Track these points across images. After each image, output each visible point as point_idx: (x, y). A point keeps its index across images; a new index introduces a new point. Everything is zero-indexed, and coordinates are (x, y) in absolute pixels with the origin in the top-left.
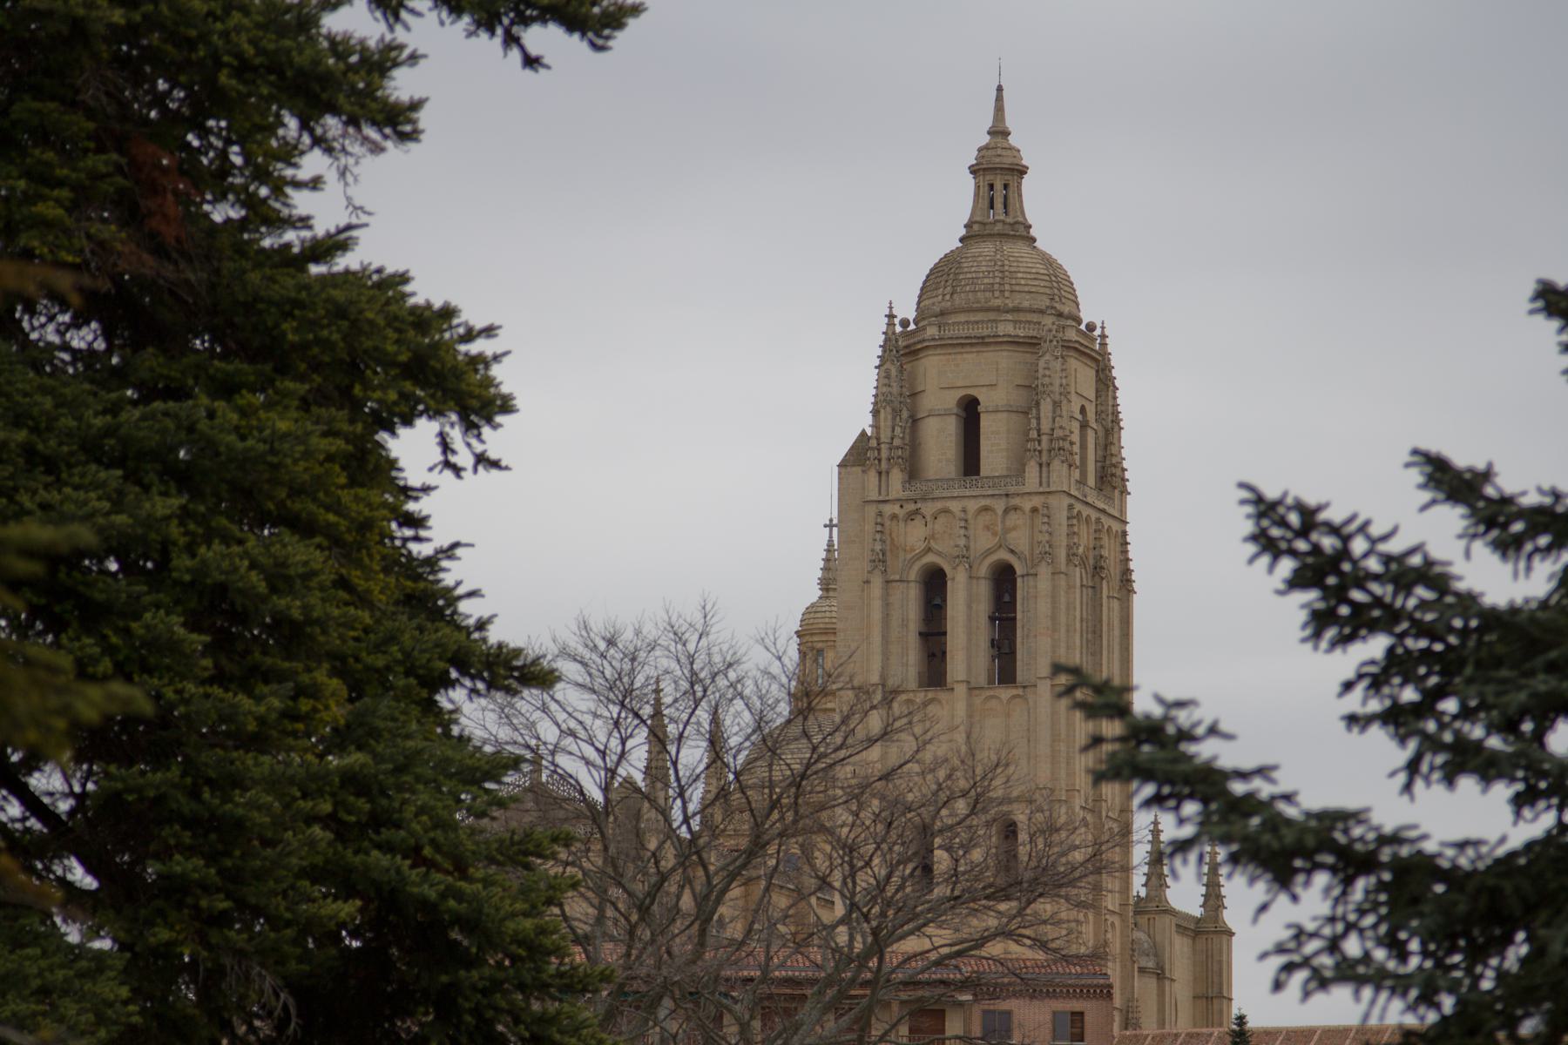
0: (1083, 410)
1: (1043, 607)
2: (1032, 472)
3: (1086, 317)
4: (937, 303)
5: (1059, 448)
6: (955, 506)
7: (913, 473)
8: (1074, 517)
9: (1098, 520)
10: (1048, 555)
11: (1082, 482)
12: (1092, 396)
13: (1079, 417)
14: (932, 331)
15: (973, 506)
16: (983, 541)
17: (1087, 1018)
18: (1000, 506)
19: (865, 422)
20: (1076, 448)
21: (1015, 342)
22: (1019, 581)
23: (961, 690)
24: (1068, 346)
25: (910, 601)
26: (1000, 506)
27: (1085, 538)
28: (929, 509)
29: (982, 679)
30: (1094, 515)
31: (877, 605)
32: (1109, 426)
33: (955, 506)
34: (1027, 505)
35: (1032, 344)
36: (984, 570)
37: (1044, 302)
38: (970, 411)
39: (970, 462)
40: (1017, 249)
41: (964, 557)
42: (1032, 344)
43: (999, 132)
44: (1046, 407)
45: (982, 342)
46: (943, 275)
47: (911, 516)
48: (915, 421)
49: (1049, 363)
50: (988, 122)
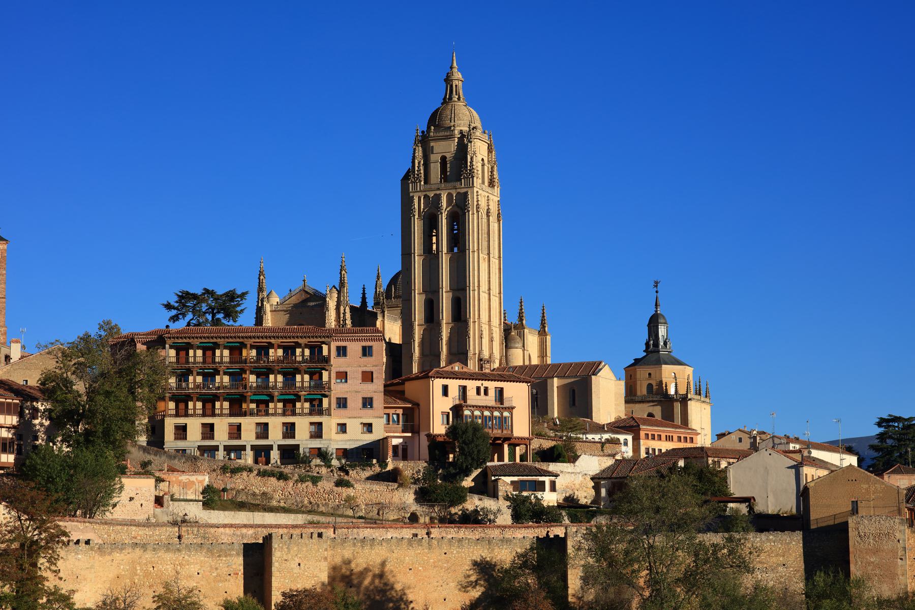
0: (483, 160)
9: (488, 197)
11: (483, 183)
12: (486, 155)
13: (481, 162)
17: (374, 348)
20: (480, 172)
22: (460, 217)
30: (487, 194)
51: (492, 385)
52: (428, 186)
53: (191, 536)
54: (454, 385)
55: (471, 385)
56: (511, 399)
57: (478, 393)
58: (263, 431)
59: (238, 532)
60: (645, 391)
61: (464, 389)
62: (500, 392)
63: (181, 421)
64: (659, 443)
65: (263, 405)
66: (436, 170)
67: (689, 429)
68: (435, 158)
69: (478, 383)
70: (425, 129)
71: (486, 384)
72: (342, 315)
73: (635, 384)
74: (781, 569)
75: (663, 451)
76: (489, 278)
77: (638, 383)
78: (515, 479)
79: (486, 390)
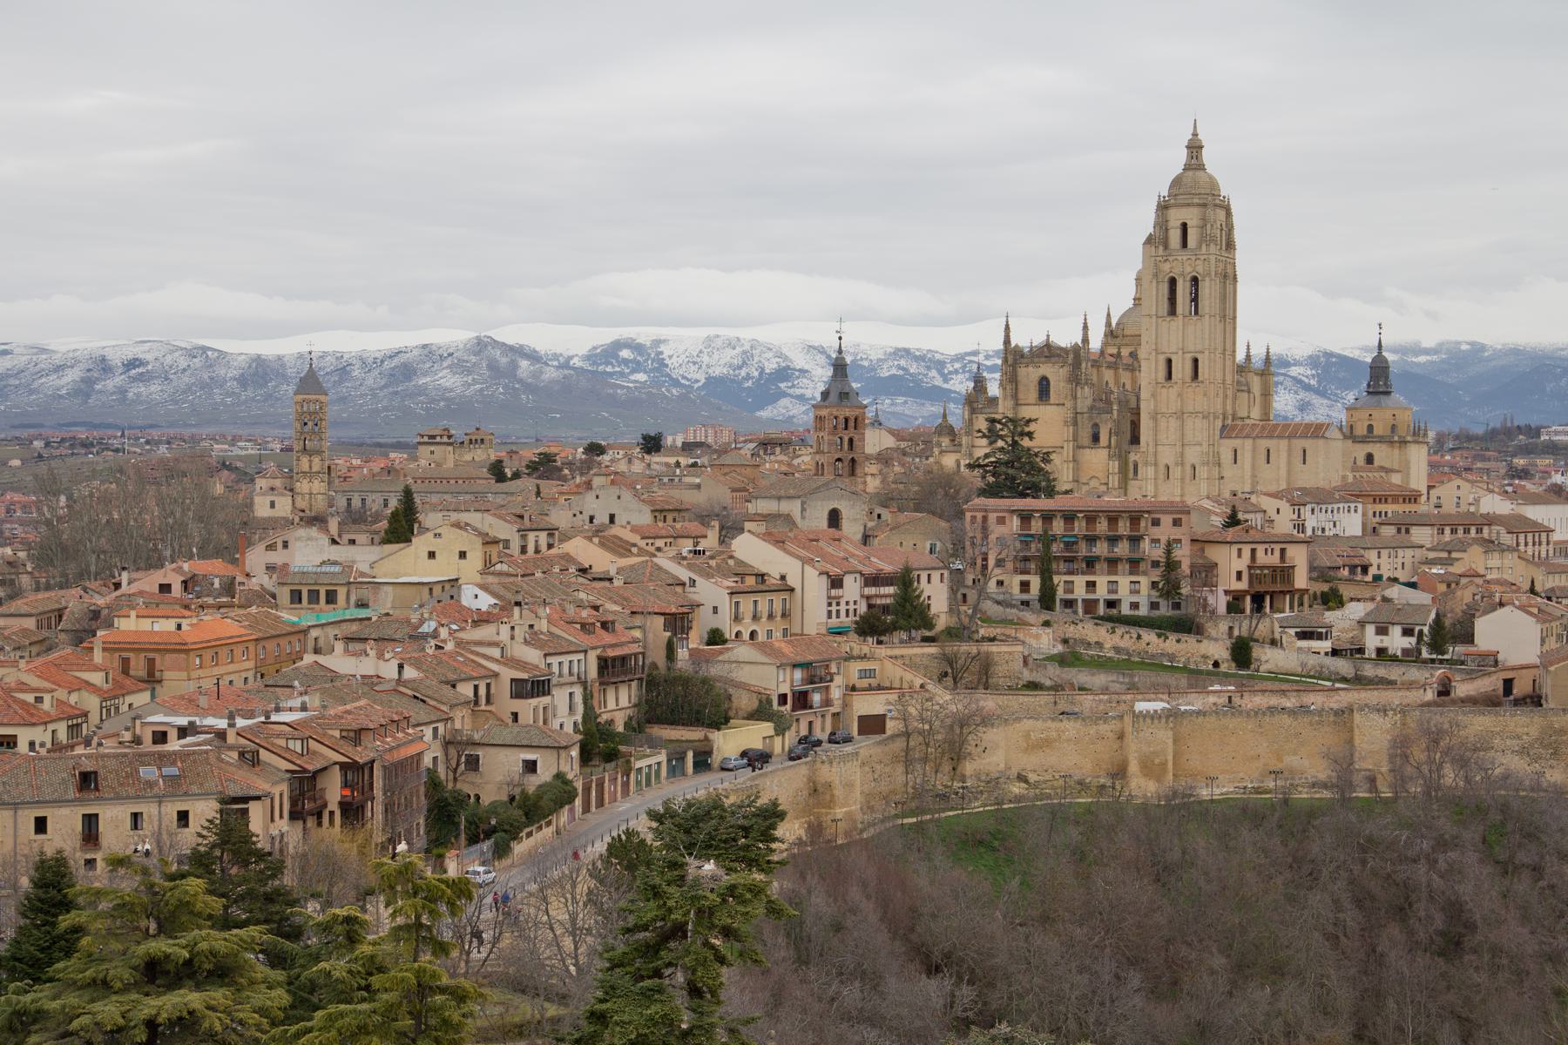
1: (1207, 291)
2: (1204, 246)
3: (1222, 194)
4: (1175, 191)
5: (1213, 240)
6: (1180, 258)
7: (1166, 247)
8: (1217, 261)
10: (1209, 274)
14: (1172, 201)
15: (1185, 258)
16: (1189, 269)
18: (1193, 258)
19: (1151, 230)
21: (1199, 205)
23: (1181, 317)
24: (1216, 205)
25: (1165, 288)
26: (1193, 258)
27: (1221, 265)
28: (1171, 258)
29: (1188, 314)
31: (1154, 289)
32: (1229, 228)
33: (1180, 258)
34: (1202, 258)
35: (1205, 205)
36: (1188, 278)
37: (1208, 191)
38: (1184, 227)
39: (1184, 244)
40: (1200, 173)
41: (1182, 275)
42: (1205, 205)
43: (1195, 134)
44: (1209, 226)
45: (1188, 205)
46: (1177, 182)
47: (1166, 261)
48: (1167, 230)
49: (1210, 212)
50: (1192, 131)
51: (1277, 548)
52: (1168, 252)
55: (1260, 549)
56: (1293, 559)
57: (1266, 554)
58: (1091, 585)
59: (1097, 698)
60: (1365, 433)
61: (1253, 551)
62: (1283, 551)
64: (1386, 506)
65: (1091, 563)
66: (1175, 237)
67: (1414, 491)
69: (1267, 546)
70: (1166, 194)
71: (1273, 546)
74: (1525, 737)
75: (1390, 515)
76: (1225, 338)
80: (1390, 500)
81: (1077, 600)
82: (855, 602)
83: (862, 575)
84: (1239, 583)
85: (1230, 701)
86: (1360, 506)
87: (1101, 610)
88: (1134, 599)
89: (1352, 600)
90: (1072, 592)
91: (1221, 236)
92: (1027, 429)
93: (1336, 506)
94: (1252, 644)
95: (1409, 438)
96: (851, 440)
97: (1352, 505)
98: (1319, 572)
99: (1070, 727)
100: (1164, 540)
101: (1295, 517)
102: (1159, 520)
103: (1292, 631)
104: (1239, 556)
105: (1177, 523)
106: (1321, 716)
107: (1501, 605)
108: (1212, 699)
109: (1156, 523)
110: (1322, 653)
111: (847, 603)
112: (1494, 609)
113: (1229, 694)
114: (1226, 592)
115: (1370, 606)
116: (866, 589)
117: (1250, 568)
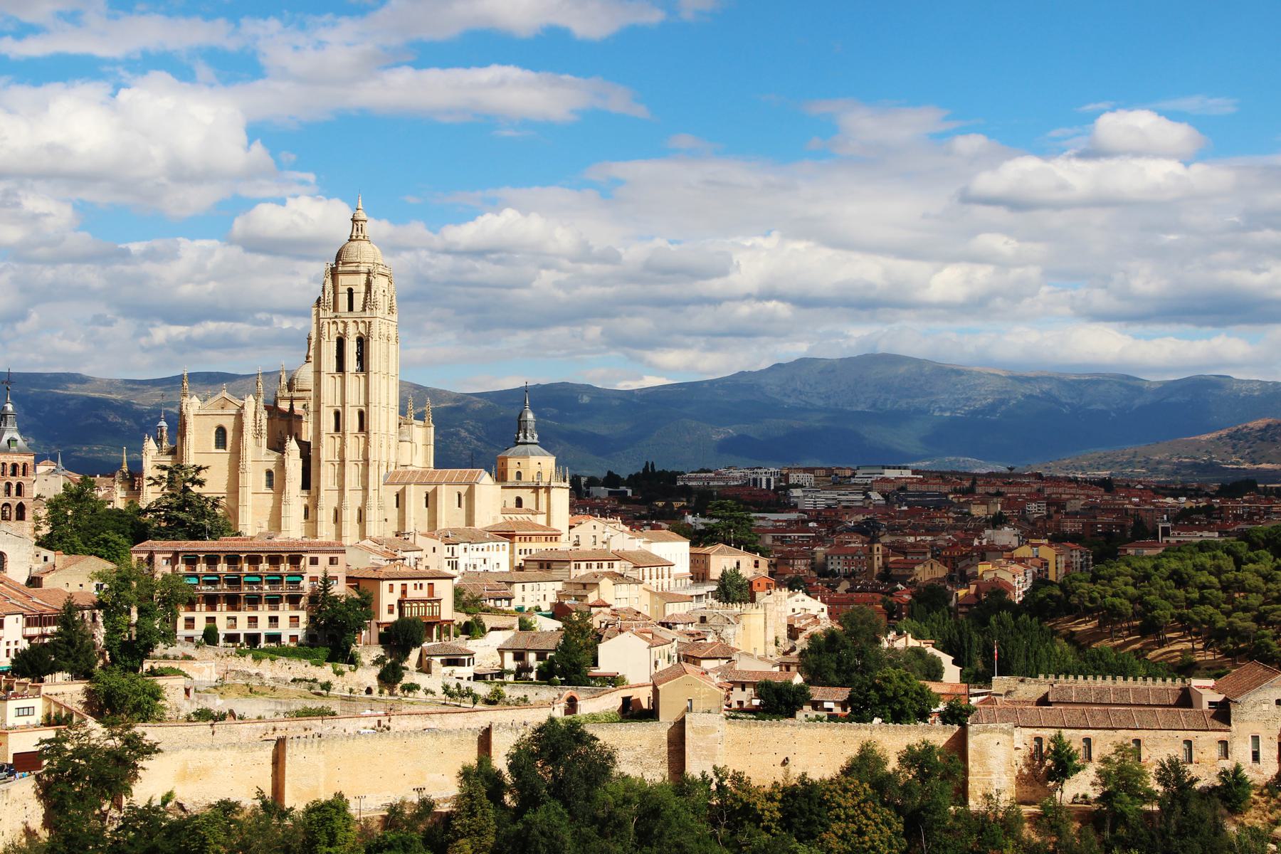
7: (335, 309)
20: (382, 304)
38: (350, 291)
39: (351, 308)
51: (425, 583)
52: (336, 314)
53: (221, 731)
54: (397, 585)
55: (410, 584)
57: (416, 589)
58: (253, 621)
60: (514, 478)
63: (190, 614)
64: (531, 544)
65: (254, 601)
66: (343, 300)
67: (555, 530)
68: (343, 289)
69: (416, 582)
71: (421, 581)
72: (258, 422)
73: (506, 470)
74: (638, 749)
75: (534, 552)
77: (509, 471)
78: (444, 658)
79: (421, 585)
80: (534, 538)
81: (239, 634)
82: (16, 642)
83: (24, 616)
84: (391, 615)
85: (379, 725)
86: (507, 544)
87: (263, 644)
88: (295, 632)
89: (492, 629)
90: (234, 626)
91: (384, 302)
92: (198, 477)
93: (485, 545)
94: (403, 671)
95: (552, 484)
96: (19, 486)
97: (501, 544)
98: (461, 602)
99: (230, 756)
100: (321, 575)
101: (449, 555)
102: (317, 558)
103: (438, 659)
104: (391, 590)
105: (332, 561)
106: (460, 735)
107: (621, 631)
108: (362, 723)
109: (314, 561)
110: (465, 679)
111: (8, 643)
112: (616, 635)
113: (378, 718)
114: (378, 625)
115: (509, 634)
116: (28, 629)
117: (400, 602)
